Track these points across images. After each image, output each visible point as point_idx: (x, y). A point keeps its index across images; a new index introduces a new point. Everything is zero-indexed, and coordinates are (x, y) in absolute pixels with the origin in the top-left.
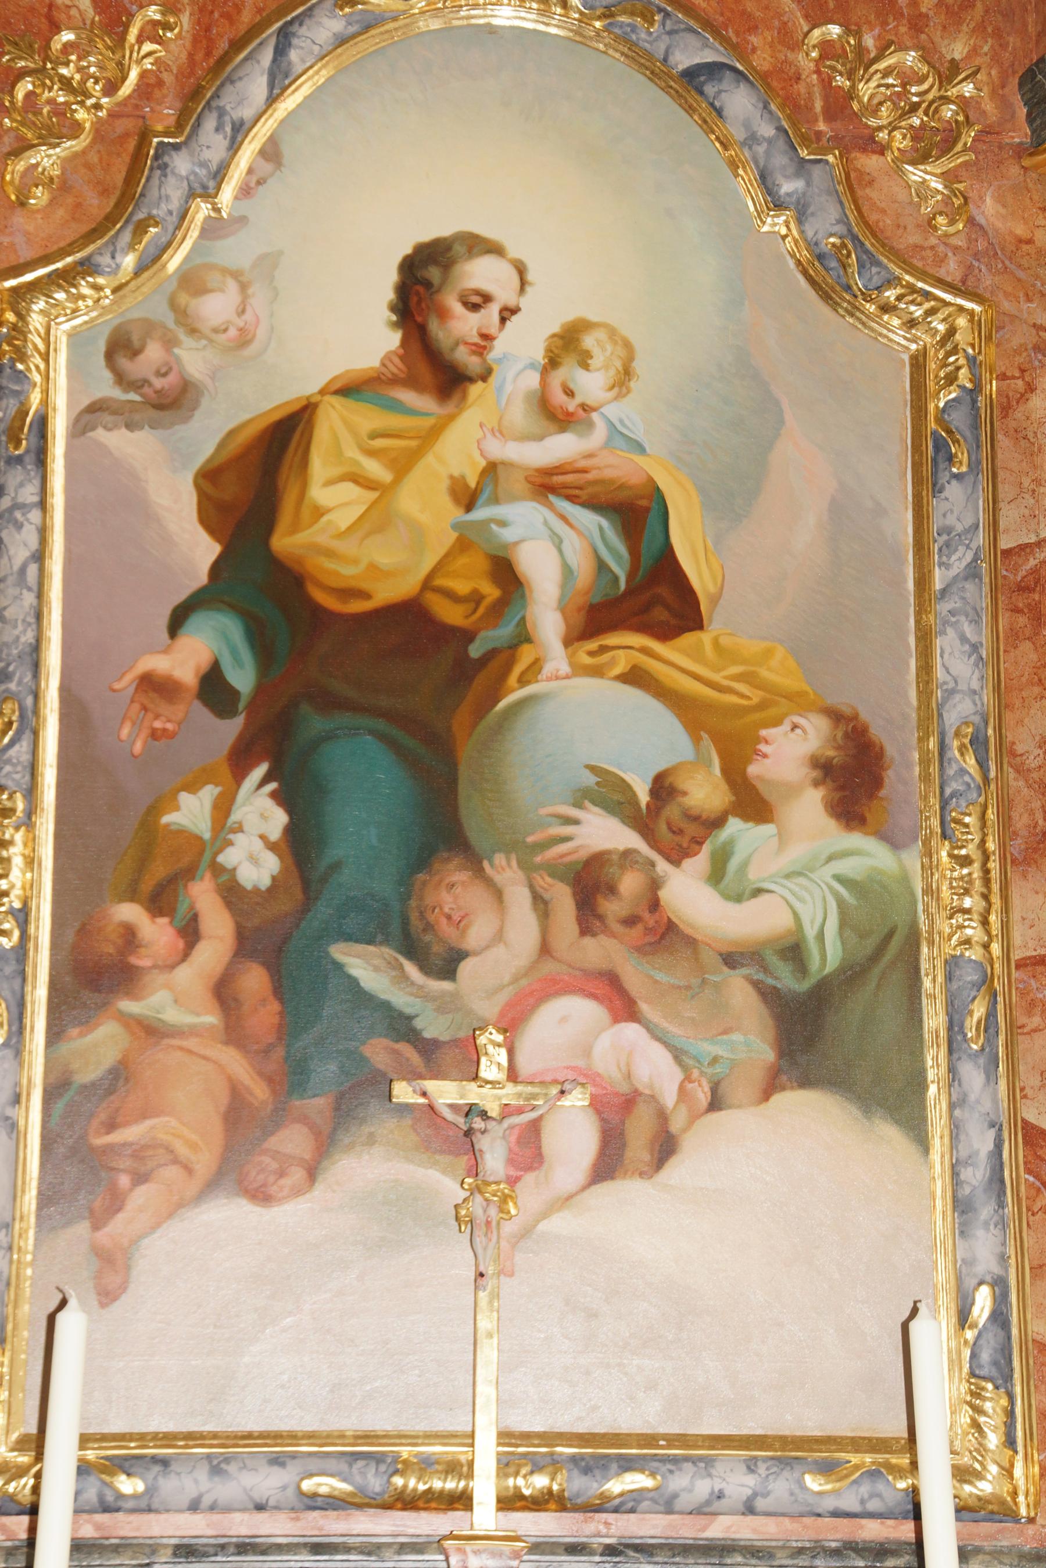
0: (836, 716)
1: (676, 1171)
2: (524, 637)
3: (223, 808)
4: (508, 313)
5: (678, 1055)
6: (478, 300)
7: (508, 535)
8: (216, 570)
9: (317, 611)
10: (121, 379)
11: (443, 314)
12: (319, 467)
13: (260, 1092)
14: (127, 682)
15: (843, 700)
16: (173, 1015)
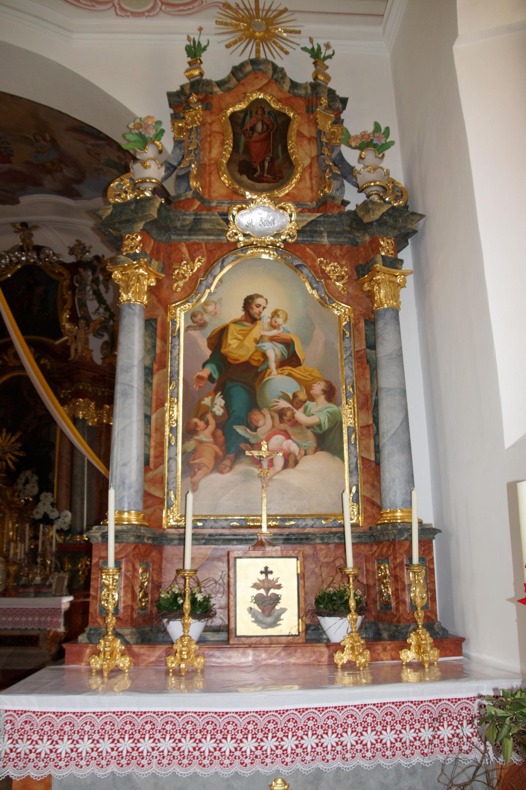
0: (326, 382)
1: (299, 467)
2: (268, 367)
3: (213, 400)
4: (264, 308)
5: (298, 445)
6: (258, 306)
7: (265, 349)
8: (211, 356)
9: (230, 364)
10: (193, 322)
11: (252, 308)
12: (229, 337)
13: (221, 453)
14: (195, 377)
15: (328, 379)
16: (204, 439)
